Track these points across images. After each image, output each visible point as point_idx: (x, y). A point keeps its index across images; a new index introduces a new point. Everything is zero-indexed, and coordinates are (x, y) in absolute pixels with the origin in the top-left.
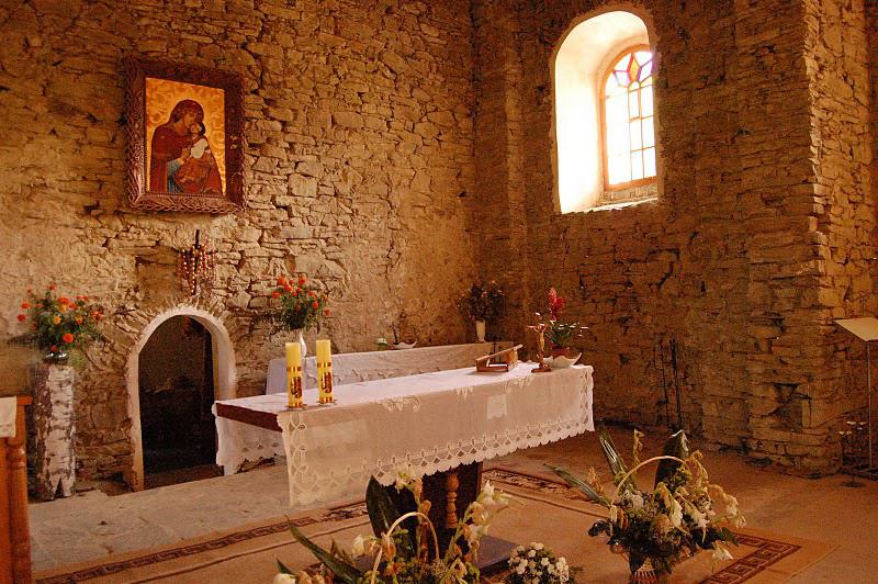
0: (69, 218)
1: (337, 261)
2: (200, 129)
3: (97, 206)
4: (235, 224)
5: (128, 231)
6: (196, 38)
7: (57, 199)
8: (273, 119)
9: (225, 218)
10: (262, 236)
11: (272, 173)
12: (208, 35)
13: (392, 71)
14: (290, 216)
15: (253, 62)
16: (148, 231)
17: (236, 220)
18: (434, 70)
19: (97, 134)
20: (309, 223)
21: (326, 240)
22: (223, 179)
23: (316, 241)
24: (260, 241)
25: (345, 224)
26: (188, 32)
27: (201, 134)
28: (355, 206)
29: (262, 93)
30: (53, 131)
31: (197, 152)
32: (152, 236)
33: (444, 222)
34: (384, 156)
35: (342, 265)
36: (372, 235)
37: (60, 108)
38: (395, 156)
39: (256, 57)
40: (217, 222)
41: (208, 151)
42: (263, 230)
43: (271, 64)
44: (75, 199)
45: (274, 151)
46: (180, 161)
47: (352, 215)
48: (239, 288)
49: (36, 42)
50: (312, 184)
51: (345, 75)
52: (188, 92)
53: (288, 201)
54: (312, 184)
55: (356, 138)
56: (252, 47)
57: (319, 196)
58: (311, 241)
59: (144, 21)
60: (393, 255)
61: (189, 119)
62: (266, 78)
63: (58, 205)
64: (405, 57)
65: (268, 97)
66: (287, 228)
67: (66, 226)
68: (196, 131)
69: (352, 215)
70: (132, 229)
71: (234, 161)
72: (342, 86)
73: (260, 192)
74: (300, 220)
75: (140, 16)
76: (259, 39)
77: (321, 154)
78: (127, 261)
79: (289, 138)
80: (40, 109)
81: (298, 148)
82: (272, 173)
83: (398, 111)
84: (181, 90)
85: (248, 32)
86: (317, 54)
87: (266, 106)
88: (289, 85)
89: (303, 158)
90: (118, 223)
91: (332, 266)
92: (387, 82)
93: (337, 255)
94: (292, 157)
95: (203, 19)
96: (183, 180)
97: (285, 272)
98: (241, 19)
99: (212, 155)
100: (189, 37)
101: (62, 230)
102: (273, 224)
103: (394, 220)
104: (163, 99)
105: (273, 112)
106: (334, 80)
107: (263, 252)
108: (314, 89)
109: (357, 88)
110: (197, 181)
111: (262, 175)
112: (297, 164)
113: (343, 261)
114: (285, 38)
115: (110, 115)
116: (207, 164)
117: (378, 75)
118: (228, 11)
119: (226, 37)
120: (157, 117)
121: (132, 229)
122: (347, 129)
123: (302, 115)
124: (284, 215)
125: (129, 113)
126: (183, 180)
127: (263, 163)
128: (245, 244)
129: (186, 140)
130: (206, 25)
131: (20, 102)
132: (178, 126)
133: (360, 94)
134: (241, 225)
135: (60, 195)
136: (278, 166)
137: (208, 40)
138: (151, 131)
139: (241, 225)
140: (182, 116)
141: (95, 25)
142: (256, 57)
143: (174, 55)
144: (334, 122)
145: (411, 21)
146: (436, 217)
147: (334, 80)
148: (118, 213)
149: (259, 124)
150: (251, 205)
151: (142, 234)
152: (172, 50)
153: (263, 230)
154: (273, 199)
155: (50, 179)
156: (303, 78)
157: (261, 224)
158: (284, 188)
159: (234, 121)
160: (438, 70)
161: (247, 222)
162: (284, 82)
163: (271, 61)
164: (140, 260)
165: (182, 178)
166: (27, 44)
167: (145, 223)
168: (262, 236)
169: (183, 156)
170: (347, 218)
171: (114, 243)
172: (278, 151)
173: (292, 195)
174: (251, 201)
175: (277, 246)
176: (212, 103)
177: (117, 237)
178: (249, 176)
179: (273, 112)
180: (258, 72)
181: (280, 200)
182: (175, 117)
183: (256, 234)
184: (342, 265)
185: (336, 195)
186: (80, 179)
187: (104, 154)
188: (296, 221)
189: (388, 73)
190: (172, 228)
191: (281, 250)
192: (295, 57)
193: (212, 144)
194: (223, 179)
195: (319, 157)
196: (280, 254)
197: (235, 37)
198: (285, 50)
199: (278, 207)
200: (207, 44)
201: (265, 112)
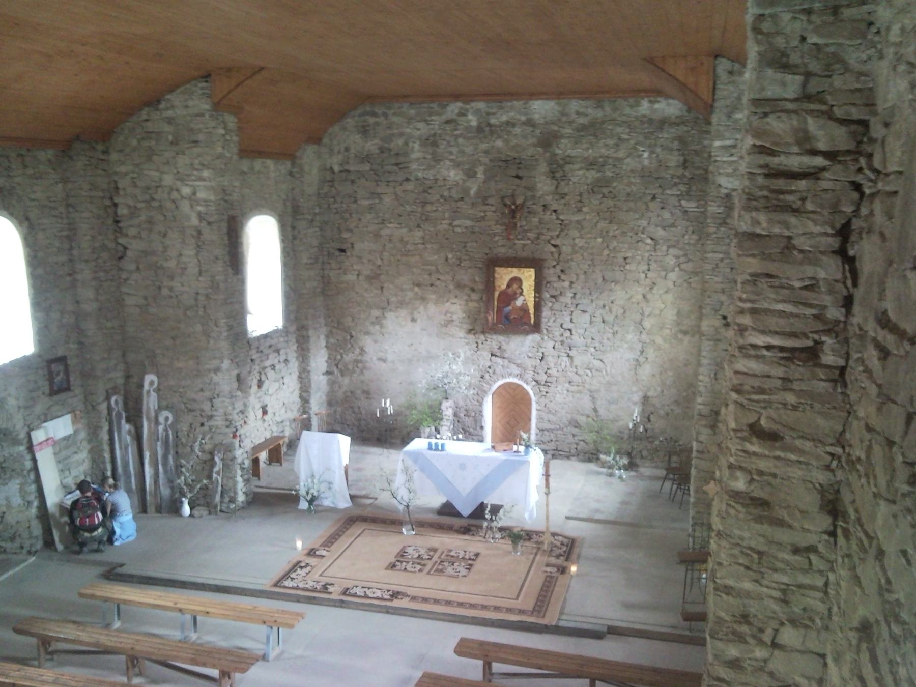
0: (462, 334)
6: (523, 242)
8: (564, 281)
12: (529, 239)
13: (652, 239)
15: (553, 249)
16: (495, 340)
18: (690, 232)
19: (475, 296)
26: (518, 239)
27: (521, 294)
28: (616, 328)
31: (519, 302)
33: (686, 339)
34: (640, 297)
36: (626, 346)
37: (459, 286)
38: (649, 296)
39: (555, 246)
43: (564, 249)
45: (562, 299)
46: (510, 308)
48: (540, 371)
49: (450, 256)
50: (587, 317)
51: (614, 248)
53: (570, 326)
54: (587, 317)
55: (618, 287)
57: (591, 322)
59: (497, 238)
60: (642, 359)
62: (561, 258)
64: (664, 228)
66: (569, 341)
71: (538, 306)
72: (612, 255)
73: (554, 321)
76: (558, 236)
79: (573, 291)
80: (451, 287)
81: (577, 296)
83: (654, 266)
85: (550, 233)
86: (596, 238)
87: (560, 273)
90: (482, 337)
91: (597, 363)
92: (648, 248)
93: (601, 357)
94: (575, 302)
95: (526, 231)
97: (568, 364)
98: (547, 226)
102: (561, 339)
103: (644, 337)
104: (503, 276)
105: (563, 277)
106: (606, 252)
107: (555, 353)
109: (623, 255)
112: (577, 305)
114: (574, 233)
115: (480, 287)
116: (524, 309)
117: (640, 244)
118: (540, 223)
119: (538, 238)
124: (567, 334)
125: (490, 284)
127: (557, 306)
129: (513, 297)
131: (444, 284)
133: (625, 259)
134: (543, 339)
137: (529, 242)
138: (497, 294)
139: (543, 339)
141: (475, 244)
142: (555, 246)
143: (511, 253)
144: (604, 279)
145: (673, 201)
146: (680, 336)
148: (483, 332)
149: (555, 285)
154: (561, 326)
155: (455, 317)
158: (568, 319)
160: (693, 232)
161: (546, 338)
166: (447, 260)
170: (610, 335)
171: (480, 346)
172: (567, 298)
176: (528, 276)
178: (546, 313)
179: (563, 277)
180: (556, 256)
182: (508, 286)
183: (551, 344)
187: (477, 305)
188: (575, 337)
189: (649, 241)
190: (507, 340)
192: (580, 242)
193: (528, 297)
195: (592, 301)
197: (543, 237)
198: (574, 239)
201: (559, 277)
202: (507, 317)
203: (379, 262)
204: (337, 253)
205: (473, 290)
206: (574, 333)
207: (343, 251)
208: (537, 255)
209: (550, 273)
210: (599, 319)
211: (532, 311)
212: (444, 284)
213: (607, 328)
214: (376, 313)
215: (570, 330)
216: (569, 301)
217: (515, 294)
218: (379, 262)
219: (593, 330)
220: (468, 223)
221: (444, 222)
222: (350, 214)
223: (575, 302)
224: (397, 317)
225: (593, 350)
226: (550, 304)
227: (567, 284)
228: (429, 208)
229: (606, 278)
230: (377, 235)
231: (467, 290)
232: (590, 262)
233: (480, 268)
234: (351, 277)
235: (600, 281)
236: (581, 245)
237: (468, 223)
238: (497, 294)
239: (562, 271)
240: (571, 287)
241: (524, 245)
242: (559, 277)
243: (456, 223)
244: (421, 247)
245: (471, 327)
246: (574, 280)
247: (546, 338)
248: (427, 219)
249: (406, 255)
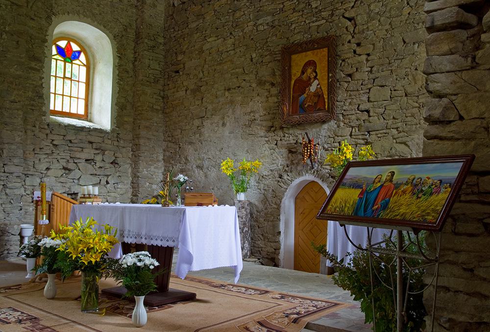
0: (262, 133)
1: (405, 143)
2: (315, 75)
3: (272, 127)
4: (336, 126)
5: (284, 137)
7: (259, 125)
9: (330, 123)
10: (351, 132)
11: (358, 90)
12: (323, 18)
14: (369, 116)
15: (349, 23)
17: (336, 123)
19: (274, 91)
20: (384, 119)
21: (397, 128)
22: (326, 100)
23: (388, 131)
24: (351, 135)
25: (413, 116)
27: (315, 78)
29: (353, 41)
30: (258, 95)
31: (313, 88)
32: (295, 138)
35: (409, 147)
39: (350, 19)
40: (325, 126)
41: (319, 86)
42: (352, 127)
43: (359, 20)
44: (264, 123)
45: (357, 76)
46: (305, 95)
47: (419, 107)
49: (254, 55)
52: (310, 56)
54: (387, 92)
56: (347, 15)
58: (384, 131)
59: (293, 26)
61: (309, 70)
62: (356, 31)
63: (259, 128)
65: (357, 42)
66: (367, 124)
67: (262, 137)
68: (313, 76)
69: (419, 107)
70: (287, 135)
73: (350, 104)
74: (376, 118)
75: (292, 24)
77: (393, 68)
78: (284, 151)
79: (369, 64)
80: (254, 85)
81: (374, 69)
82: (358, 90)
84: (306, 56)
88: (371, 28)
89: (378, 75)
90: (281, 133)
93: (404, 139)
94: (372, 76)
96: (306, 106)
99: (320, 88)
100: (314, 24)
101: (260, 138)
105: (359, 50)
108: (390, 24)
110: (313, 104)
111: (352, 93)
113: (409, 143)
115: (279, 79)
119: (332, 15)
120: (295, 75)
121: (287, 135)
122: (414, 43)
123: (379, 45)
124: (365, 116)
126: (306, 106)
127: (353, 85)
128: (341, 138)
130: (322, 13)
131: (248, 84)
132: (304, 77)
134: (338, 126)
135: (260, 123)
136: (362, 84)
138: (293, 82)
139: (338, 126)
140: (306, 71)
144: (405, 42)
147: (407, 10)
148: (282, 128)
150: (345, 113)
151: (291, 137)
152: (306, 36)
153: (352, 127)
155: (257, 116)
156: (382, 19)
157: (350, 124)
158: (365, 98)
159: (332, 67)
161: (342, 124)
162: (368, 28)
163: (359, 18)
164: (290, 152)
165: (306, 104)
167: (291, 131)
168: (351, 132)
169: (306, 92)
171: (279, 142)
172: (363, 75)
173: (371, 102)
174: (345, 110)
175: (361, 137)
176: (320, 56)
177: (281, 140)
178: (341, 95)
179: (359, 50)
181: (362, 107)
182: (303, 73)
184: (409, 147)
185: (406, 95)
186: (267, 114)
187: (276, 100)
191: (363, 139)
194: (326, 100)
196: (363, 142)
198: (369, 6)
199: (362, 111)
200: (322, 24)
202: (302, 107)
203: (201, 75)
204: (174, 74)
205: (273, 85)
206: (371, 114)
207: (177, 72)
208: (332, 32)
209: (345, 50)
210: (402, 93)
211: (326, 97)
212: (248, 84)
213: (410, 101)
214: (197, 122)
215: (368, 111)
216: (365, 76)
217: (310, 79)
218: (201, 75)
219: (394, 107)
220: (269, 19)
221: (249, 24)
222: (184, 38)
223: (372, 76)
224: (212, 124)
225: (395, 132)
226: (346, 85)
227: (364, 57)
228: (238, 14)
229: (407, 40)
230: (201, 51)
231: (267, 86)
232: (388, 27)
233: (279, 61)
234: (182, 93)
235: (400, 46)
236: (377, 10)
237: (269, 19)
238: (293, 82)
239: (358, 45)
240: (367, 60)
241: (318, 26)
242: (355, 52)
243: (259, 22)
244: (232, 52)
245: (270, 124)
246: (370, 51)
247: (342, 124)
248: (236, 26)
249: (220, 64)
